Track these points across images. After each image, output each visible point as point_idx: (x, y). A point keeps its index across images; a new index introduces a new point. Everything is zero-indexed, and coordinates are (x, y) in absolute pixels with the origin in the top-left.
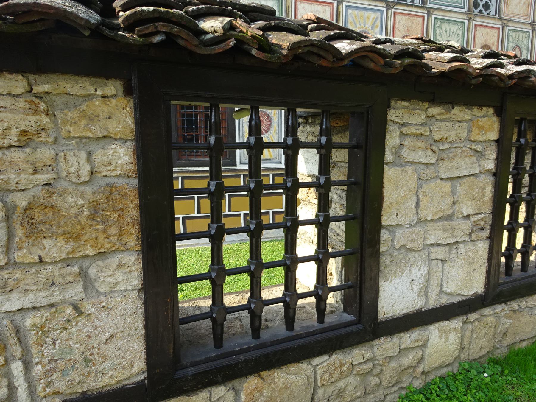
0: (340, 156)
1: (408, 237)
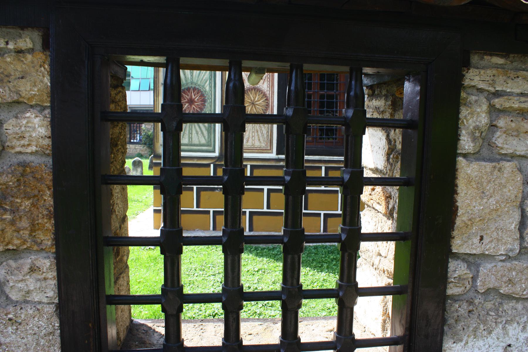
1: (502, 276)
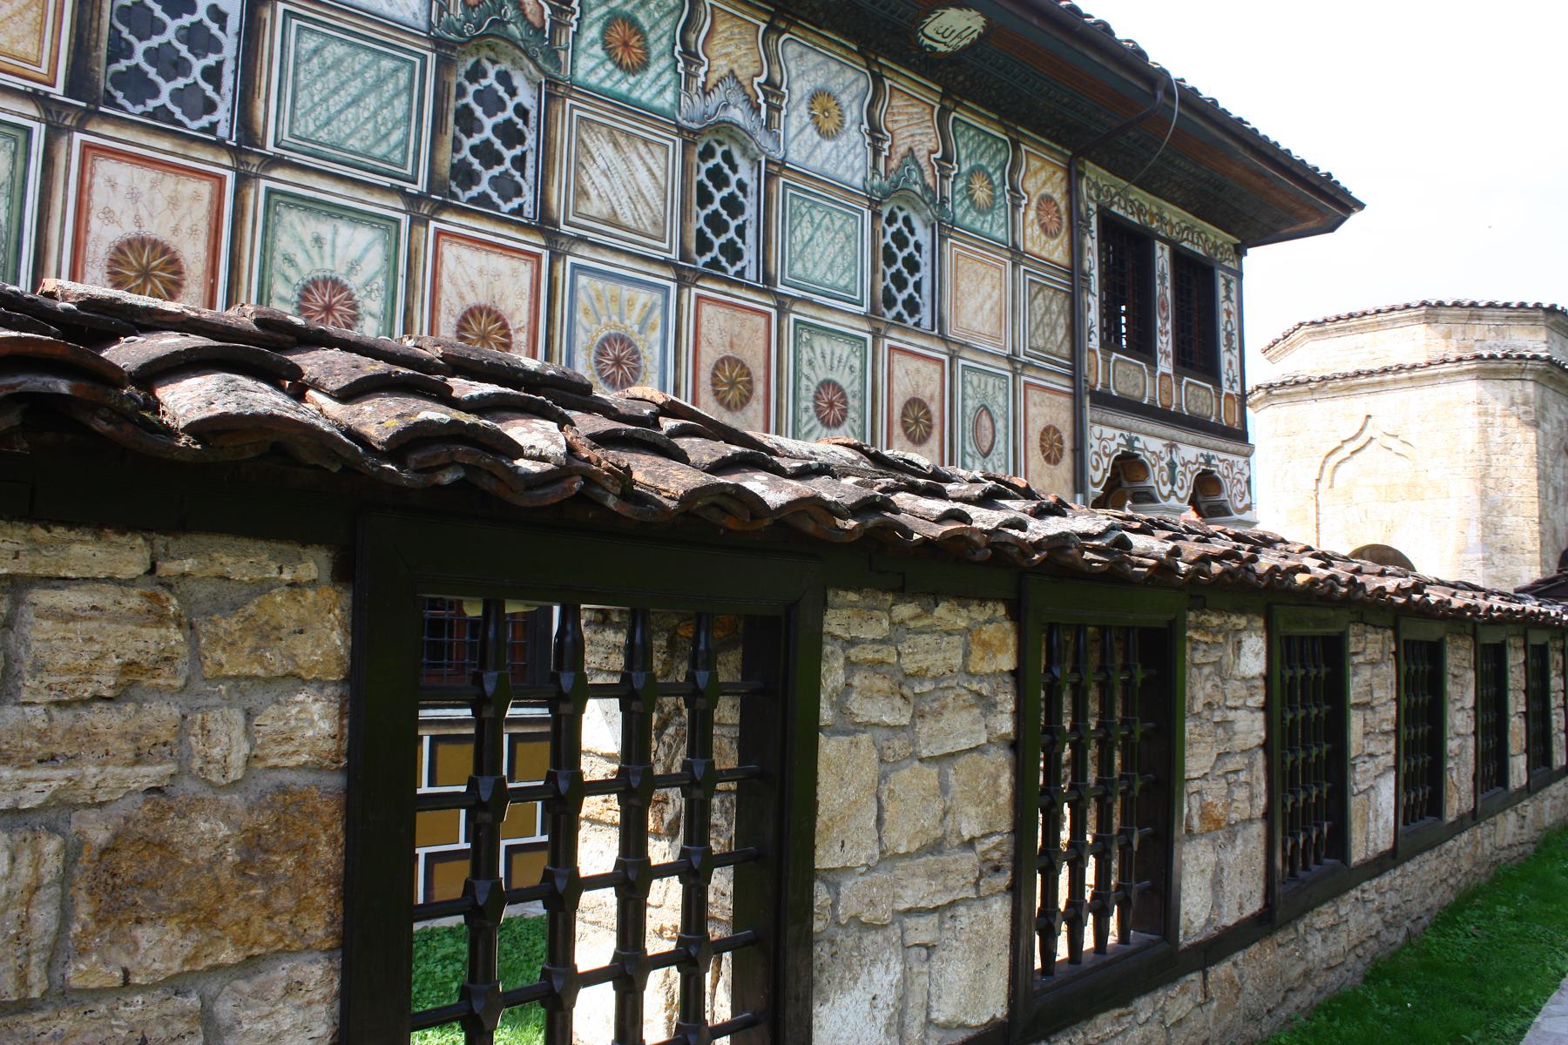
0: (727, 712)
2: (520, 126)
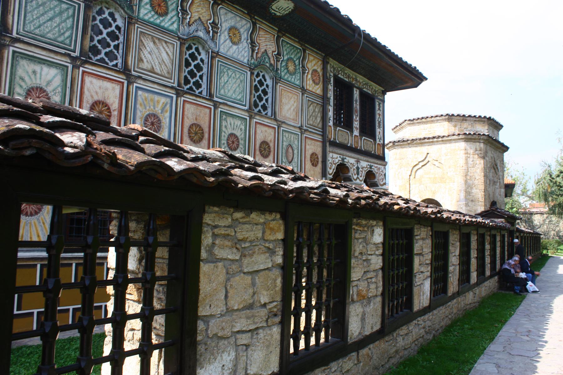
0: (162, 253)
1: (219, 326)
2: (118, 33)
